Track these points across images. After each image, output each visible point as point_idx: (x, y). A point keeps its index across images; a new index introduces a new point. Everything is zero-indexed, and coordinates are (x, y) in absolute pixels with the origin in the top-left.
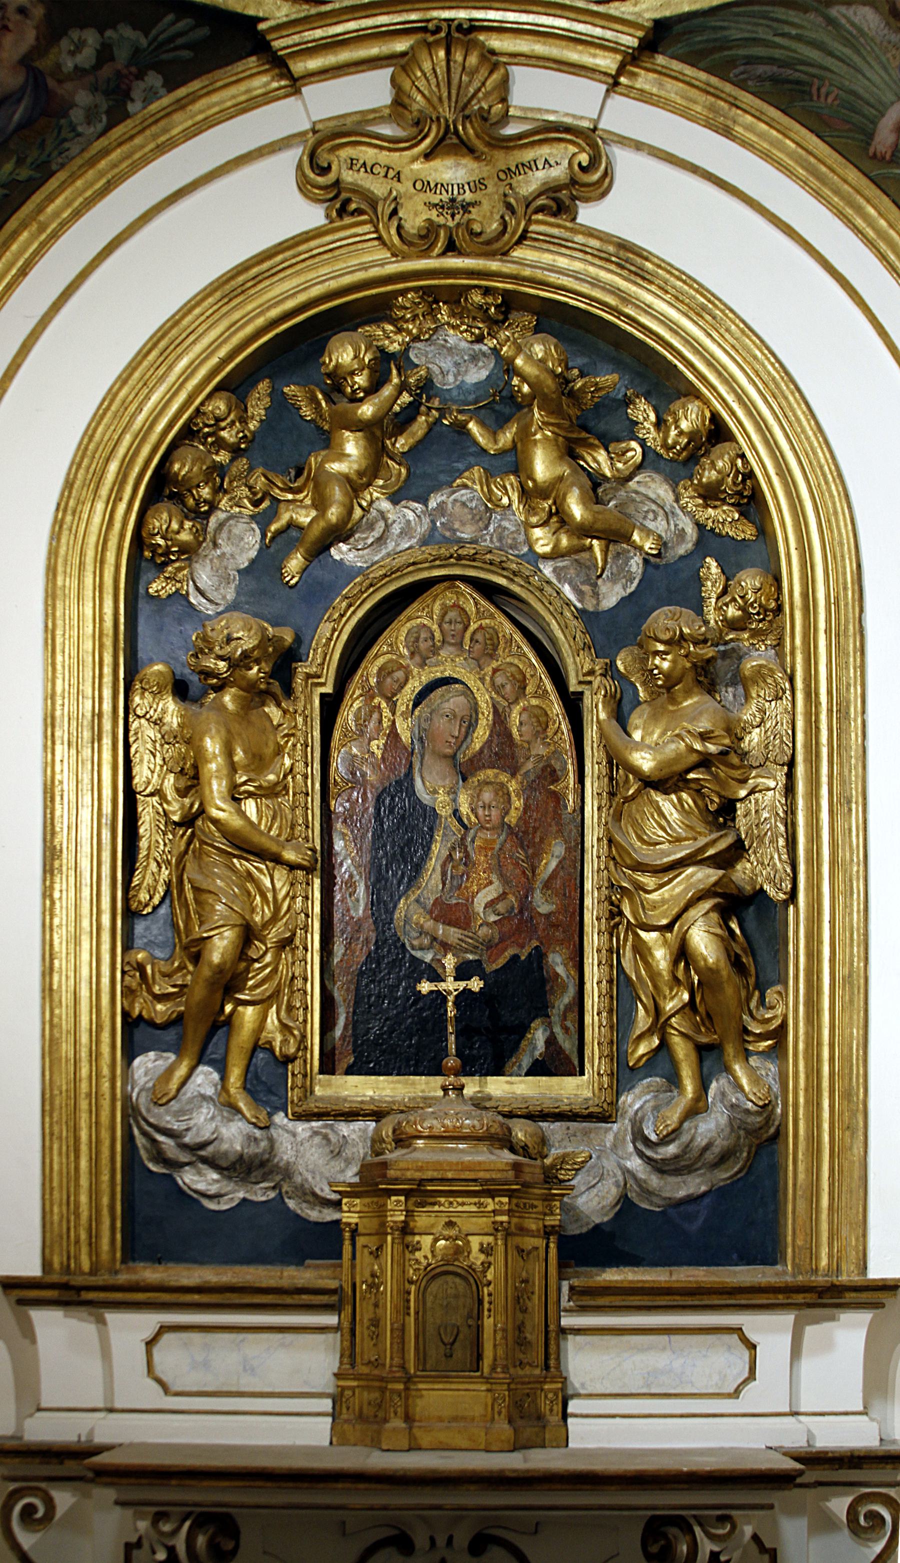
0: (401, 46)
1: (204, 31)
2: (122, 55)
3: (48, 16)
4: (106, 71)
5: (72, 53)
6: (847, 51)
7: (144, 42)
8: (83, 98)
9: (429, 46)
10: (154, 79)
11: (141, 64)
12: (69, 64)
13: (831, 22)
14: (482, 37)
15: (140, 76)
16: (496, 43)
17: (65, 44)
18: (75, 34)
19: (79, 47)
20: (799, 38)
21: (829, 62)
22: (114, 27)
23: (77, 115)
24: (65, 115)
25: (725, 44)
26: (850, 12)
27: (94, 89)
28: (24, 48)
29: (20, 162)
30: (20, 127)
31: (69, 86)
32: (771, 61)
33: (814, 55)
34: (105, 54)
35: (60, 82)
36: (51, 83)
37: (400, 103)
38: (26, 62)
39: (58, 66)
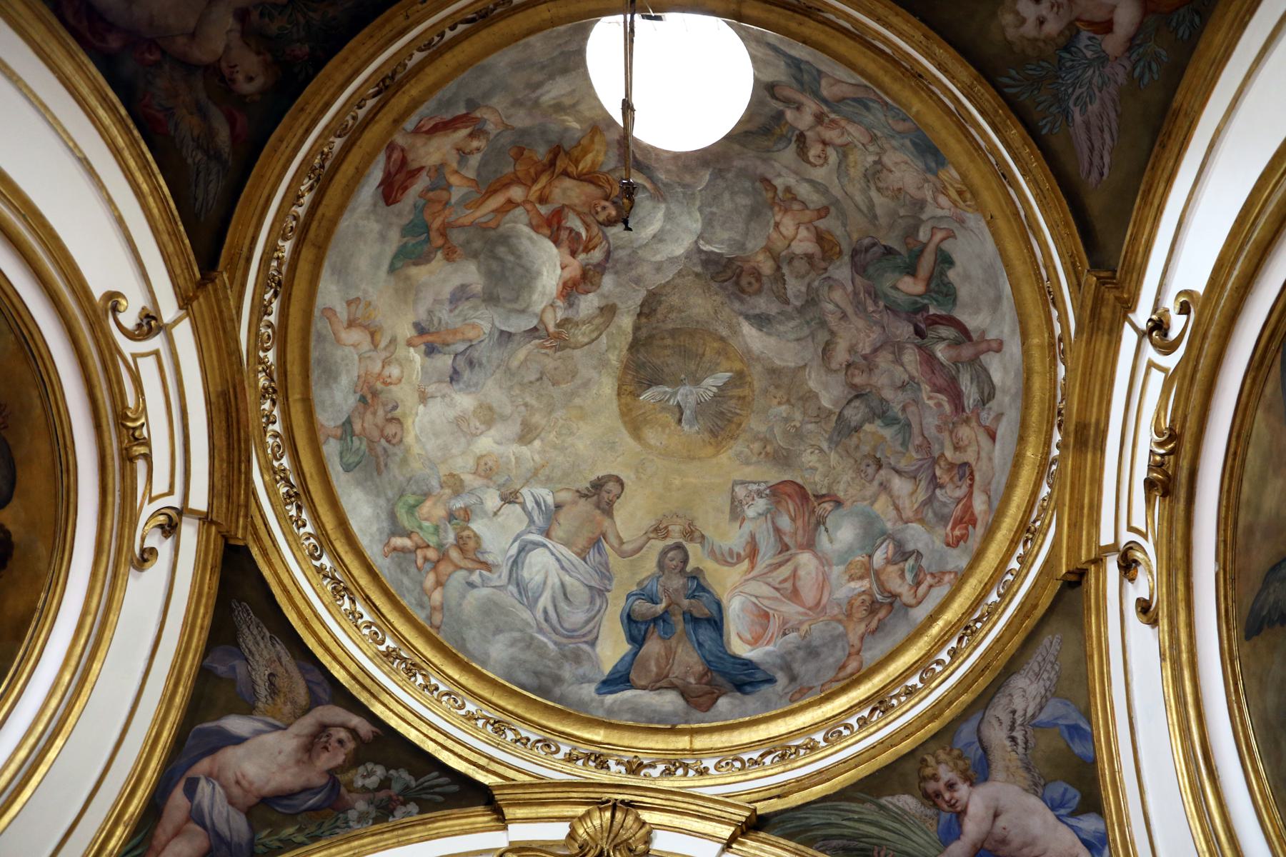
0: (581, 810)
1: (455, 788)
2: (396, 787)
3: (356, 750)
4: (382, 794)
5: (364, 777)
6: (897, 826)
7: (413, 784)
8: (361, 805)
9: (600, 810)
10: (413, 807)
11: (407, 796)
12: (359, 783)
13: (882, 807)
14: (640, 812)
15: (404, 804)
16: (646, 816)
17: (361, 770)
18: (370, 766)
19: (369, 775)
20: (860, 821)
21: (884, 834)
22: (396, 769)
23: (352, 814)
24: (345, 811)
25: (809, 828)
26: (894, 800)
27: (370, 802)
28: (333, 764)
29: (300, 830)
30: (311, 809)
31: (354, 796)
32: (842, 837)
33: (873, 830)
34: (385, 784)
35: (349, 791)
36: (343, 790)
37: (572, 836)
38: (332, 773)
39: (352, 782)
